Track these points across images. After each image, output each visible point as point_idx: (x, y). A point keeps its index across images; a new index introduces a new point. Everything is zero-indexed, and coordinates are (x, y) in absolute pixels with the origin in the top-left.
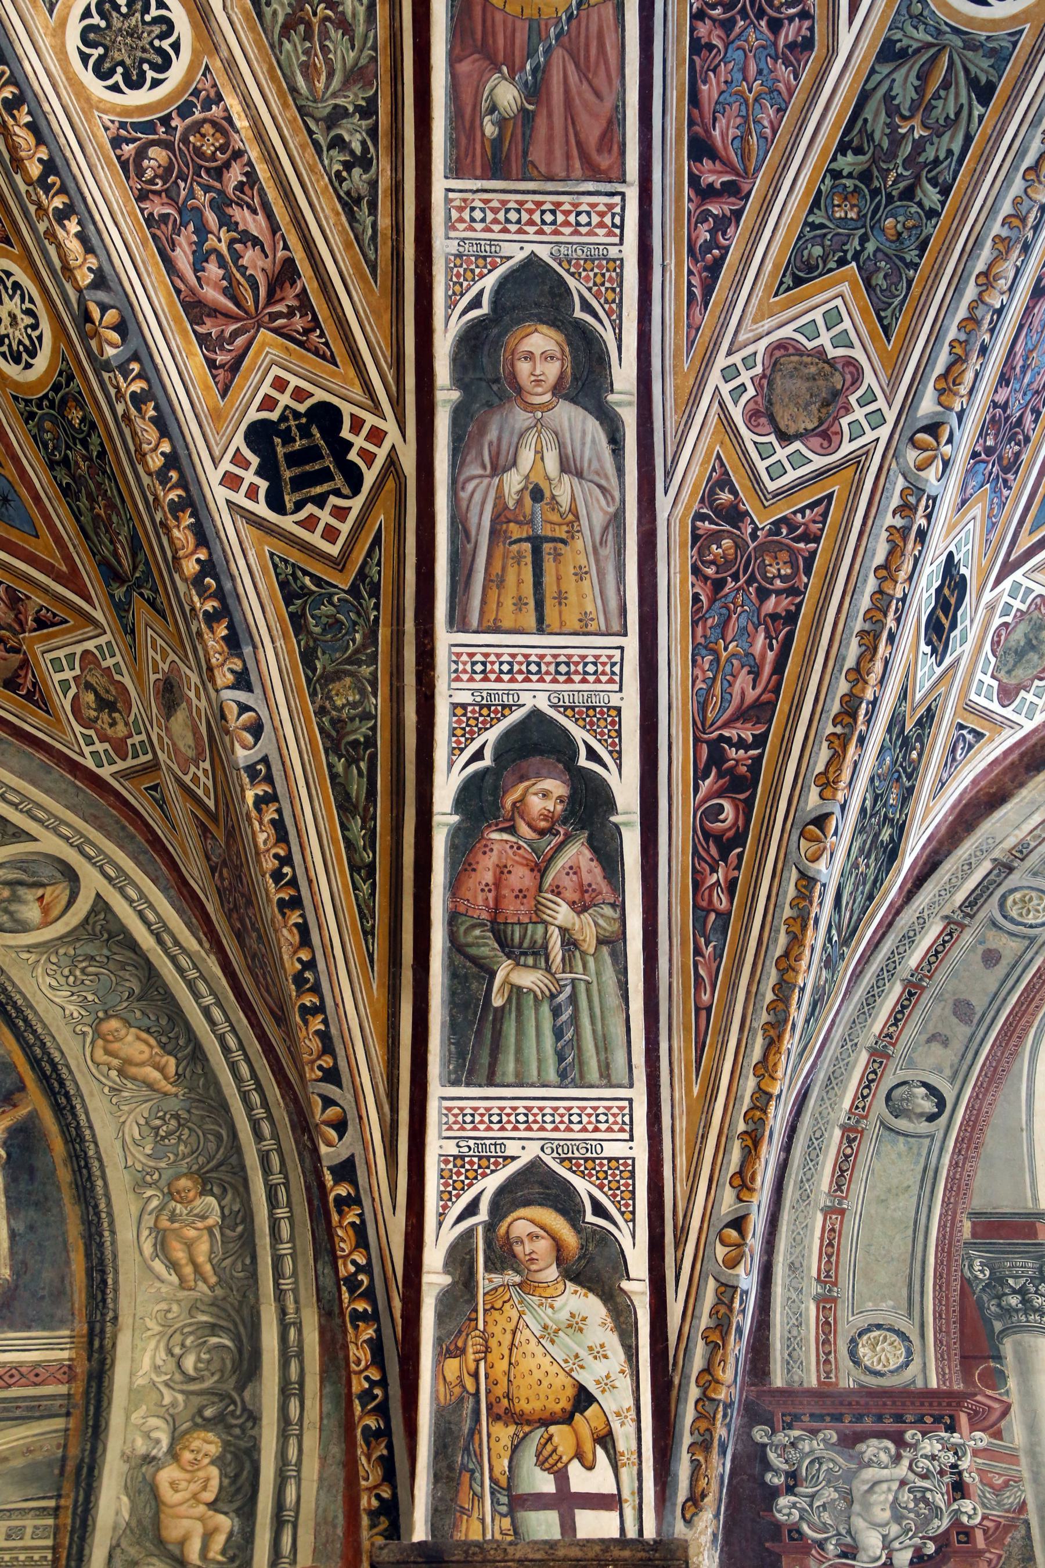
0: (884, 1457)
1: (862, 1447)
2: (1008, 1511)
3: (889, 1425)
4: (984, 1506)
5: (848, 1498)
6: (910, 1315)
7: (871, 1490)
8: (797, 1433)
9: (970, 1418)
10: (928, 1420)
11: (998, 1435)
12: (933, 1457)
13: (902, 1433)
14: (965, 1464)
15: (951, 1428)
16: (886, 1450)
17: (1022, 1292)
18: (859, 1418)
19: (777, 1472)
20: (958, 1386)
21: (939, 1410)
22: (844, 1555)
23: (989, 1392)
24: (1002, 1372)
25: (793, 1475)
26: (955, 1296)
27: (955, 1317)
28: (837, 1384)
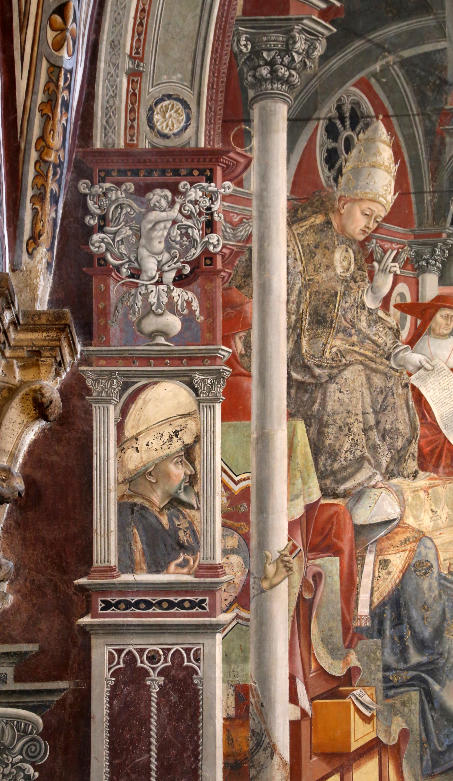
0: (164, 203)
1: (150, 195)
2: (239, 241)
3: (170, 178)
4: (224, 238)
5: (138, 234)
6: (192, 87)
7: (153, 228)
8: (108, 185)
9: (224, 170)
10: (196, 173)
11: (240, 184)
12: (196, 202)
13: (177, 183)
14: (216, 207)
15: (210, 180)
16: (166, 197)
17: (272, 63)
18: (150, 173)
19: (93, 215)
20: (218, 146)
21: (200, 164)
22: (132, 276)
23: (239, 150)
24: (249, 132)
25: (103, 218)
28: (137, 145)
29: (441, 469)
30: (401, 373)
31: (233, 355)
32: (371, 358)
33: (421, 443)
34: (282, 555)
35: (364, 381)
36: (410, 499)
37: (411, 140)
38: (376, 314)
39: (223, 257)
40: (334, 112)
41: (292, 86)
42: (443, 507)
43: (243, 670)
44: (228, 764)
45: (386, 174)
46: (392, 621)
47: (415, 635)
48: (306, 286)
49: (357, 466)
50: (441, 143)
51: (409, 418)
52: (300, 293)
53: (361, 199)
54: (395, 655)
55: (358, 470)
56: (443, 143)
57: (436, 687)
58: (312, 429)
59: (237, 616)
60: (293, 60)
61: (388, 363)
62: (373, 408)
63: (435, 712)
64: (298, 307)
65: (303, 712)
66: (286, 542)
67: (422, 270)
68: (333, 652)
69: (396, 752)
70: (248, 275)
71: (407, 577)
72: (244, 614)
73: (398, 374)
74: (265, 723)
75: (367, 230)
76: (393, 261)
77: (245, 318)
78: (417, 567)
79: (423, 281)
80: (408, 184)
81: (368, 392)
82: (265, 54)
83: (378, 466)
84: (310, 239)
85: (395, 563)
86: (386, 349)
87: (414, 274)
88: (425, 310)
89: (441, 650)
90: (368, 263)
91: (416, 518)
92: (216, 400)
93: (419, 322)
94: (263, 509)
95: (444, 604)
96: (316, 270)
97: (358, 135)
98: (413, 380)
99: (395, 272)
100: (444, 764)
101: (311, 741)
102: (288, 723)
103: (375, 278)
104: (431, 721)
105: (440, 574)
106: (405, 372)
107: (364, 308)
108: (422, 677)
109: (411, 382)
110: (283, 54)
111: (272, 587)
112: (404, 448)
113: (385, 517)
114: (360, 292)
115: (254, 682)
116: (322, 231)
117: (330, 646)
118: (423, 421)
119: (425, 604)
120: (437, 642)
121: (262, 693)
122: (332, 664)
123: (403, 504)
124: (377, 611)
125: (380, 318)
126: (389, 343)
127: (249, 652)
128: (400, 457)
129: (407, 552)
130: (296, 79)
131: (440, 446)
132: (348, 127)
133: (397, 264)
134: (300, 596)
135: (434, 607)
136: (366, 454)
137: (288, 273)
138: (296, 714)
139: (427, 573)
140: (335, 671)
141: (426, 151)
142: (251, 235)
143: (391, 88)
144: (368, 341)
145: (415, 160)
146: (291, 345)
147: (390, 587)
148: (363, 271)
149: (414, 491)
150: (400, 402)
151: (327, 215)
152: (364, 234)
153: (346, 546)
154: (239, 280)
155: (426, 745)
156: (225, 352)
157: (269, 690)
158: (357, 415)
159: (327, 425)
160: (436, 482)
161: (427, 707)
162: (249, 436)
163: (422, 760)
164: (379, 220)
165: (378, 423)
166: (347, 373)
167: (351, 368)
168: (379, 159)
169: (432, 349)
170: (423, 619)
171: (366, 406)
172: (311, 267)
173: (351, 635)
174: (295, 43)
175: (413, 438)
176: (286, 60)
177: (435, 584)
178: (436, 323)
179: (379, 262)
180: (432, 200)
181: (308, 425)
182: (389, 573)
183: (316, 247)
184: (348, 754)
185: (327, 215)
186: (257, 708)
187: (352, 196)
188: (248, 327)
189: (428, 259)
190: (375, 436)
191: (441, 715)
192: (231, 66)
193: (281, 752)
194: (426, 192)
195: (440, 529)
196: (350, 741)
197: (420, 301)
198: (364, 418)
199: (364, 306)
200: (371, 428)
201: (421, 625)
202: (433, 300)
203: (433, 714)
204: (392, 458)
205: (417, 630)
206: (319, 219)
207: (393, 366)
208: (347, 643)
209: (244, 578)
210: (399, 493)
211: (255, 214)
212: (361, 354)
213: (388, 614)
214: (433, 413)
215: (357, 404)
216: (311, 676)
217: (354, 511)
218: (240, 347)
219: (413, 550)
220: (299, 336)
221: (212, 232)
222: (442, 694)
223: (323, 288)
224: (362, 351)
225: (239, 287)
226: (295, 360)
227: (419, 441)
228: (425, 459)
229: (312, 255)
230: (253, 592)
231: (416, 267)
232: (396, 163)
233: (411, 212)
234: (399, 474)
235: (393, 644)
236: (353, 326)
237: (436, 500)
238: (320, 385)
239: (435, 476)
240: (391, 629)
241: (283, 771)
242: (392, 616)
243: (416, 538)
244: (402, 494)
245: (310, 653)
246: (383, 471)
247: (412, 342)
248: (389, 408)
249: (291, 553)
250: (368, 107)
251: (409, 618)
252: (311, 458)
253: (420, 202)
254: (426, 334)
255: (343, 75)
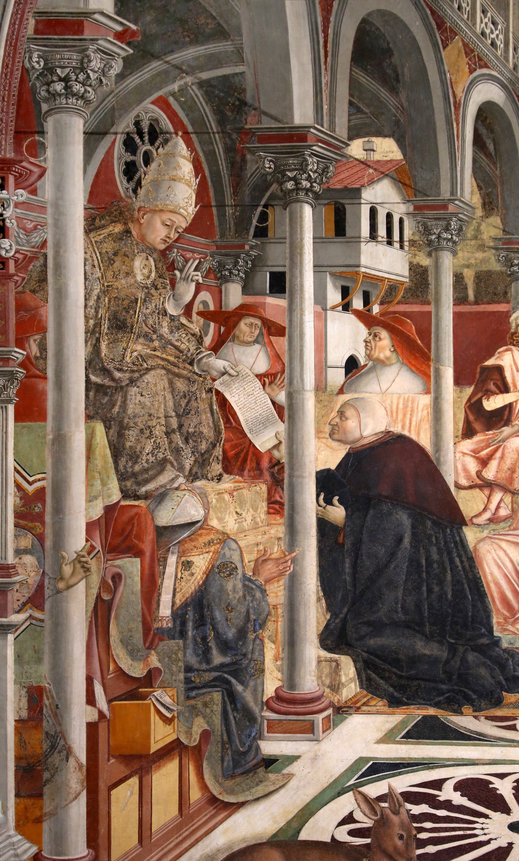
2: (33, 247)
4: (18, 243)
9: (16, 179)
11: (34, 192)
17: (66, 80)
23: (32, 160)
24: (43, 144)
26: (16, 83)
27: (14, 100)
29: (246, 473)
30: (205, 378)
31: (28, 357)
32: (174, 363)
33: (225, 447)
34: (79, 556)
35: (167, 385)
36: (214, 501)
37: (211, 155)
38: (179, 320)
39: (16, 262)
40: (132, 128)
41: (87, 102)
42: (248, 510)
43: (36, 671)
44: (20, 766)
45: (187, 187)
46: (195, 622)
47: (218, 636)
48: (105, 291)
49: (159, 469)
50: (242, 160)
51: (213, 421)
52: (99, 298)
53: (161, 211)
54: (198, 655)
55: (161, 472)
56: (244, 160)
57: (240, 688)
58: (112, 432)
59: (31, 617)
60: (88, 77)
61: (191, 368)
62: (175, 412)
63: (237, 712)
64: (97, 312)
65: (101, 714)
66: (84, 543)
67: (226, 280)
68: (133, 653)
69: (198, 753)
70: (43, 280)
71: (211, 578)
72: (38, 614)
73: (201, 379)
74: (60, 725)
75: (167, 239)
76: (195, 270)
77: (40, 321)
78: (221, 569)
79: (226, 290)
80: (209, 198)
81: (171, 396)
82: (59, 71)
83: (181, 469)
84: (109, 247)
85: (198, 564)
86: (189, 355)
87: (217, 283)
88: (228, 318)
89: (244, 651)
90: (169, 271)
91: (220, 520)
92: (9, 401)
93: (222, 329)
94: (59, 509)
95: (248, 605)
96: (115, 276)
97: (157, 150)
98: (218, 385)
99: (197, 281)
100: (245, 765)
101: (109, 743)
102: (85, 725)
103: (177, 286)
104: (233, 722)
105: (244, 575)
106: (208, 378)
107: (166, 315)
108: (224, 678)
109: (215, 387)
110: (78, 71)
111: (69, 587)
112: (208, 451)
113: (188, 518)
114: (162, 298)
115: (48, 683)
116: (121, 239)
117: (129, 647)
118: (228, 425)
119: (229, 605)
120: (241, 643)
121: (57, 694)
122: (131, 665)
123: (207, 506)
124: (179, 612)
125: (182, 324)
126: (192, 349)
127: (43, 653)
128: (204, 460)
129: (211, 554)
130: (91, 95)
131: (245, 450)
132: (147, 141)
133: (199, 273)
134: (99, 597)
135: (238, 608)
136: (169, 457)
137: (86, 279)
138: (92, 715)
139: (231, 574)
140: (135, 673)
141: (227, 167)
142: (46, 241)
143: (190, 107)
144: (170, 346)
145: (216, 175)
146: (90, 348)
147: (193, 588)
148: (164, 278)
149: (219, 494)
150: (203, 406)
151: (126, 224)
152: (164, 244)
153: (147, 547)
154: (33, 284)
155: (227, 746)
156: (19, 354)
157: (65, 692)
158: (159, 418)
159: (128, 428)
160: (241, 485)
161: (229, 708)
162: (44, 437)
163: (223, 761)
164: (180, 230)
165: (180, 426)
166: (149, 377)
167: (153, 372)
168: (180, 173)
169: (236, 356)
170: (227, 620)
171: (169, 410)
172: (110, 274)
173: (152, 635)
174: (90, 61)
175: (218, 442)
176: (81, 77)
177: (240, 585)
178: (241, 331)
179: (181, 271)
180: (234, 214)
181: (108, 428)
182: (192, 574)
183: (115, 254)
184: (147, 756)
185: (126, 224)
186: (51, 710)
187: (152, 207)
188: (43, 330)
189: (231, 269)
190: (178, 439)
191: (243, 716)
192: (22, 81)
193: (77, 755)
194: (228, 206)
195: (245, 531)
196: (149, 743)
197: (223, 309)
198: (166, 421)
199: (165, 313)
200: (173, 431)
201: (225, 625)
202: (237, 308)
203: (235, 715)
204: (195, 461)
205: (220, 631)
206: (118, 228)
207: (197, 371)
208: (147, 645)
209: (39, 578)
210: (203, 496)
211: (50, 221)
212: (163, 359)
213: (190, 615)
214: (238, 418)
215: (159, 407)
216: (109, 677)
217: (156, 513)
218: (35, 350)
219: (217, 552)
220: (98, 340)
221: (4, 237)
222: (245, 694)
223: (122, 295)
224: (164, 356)
225: (33, 291)
226: (93, 363)
227: (224, 445)
228: (230, 462)
229: (111, 262)
230: (47, 592)
231: (219, 276)
232: (197, 177)
233: (212, 223)
234: (203, 476)
235: (195, 645)
236: (155, 332)
237: (241, 503)
238: (120, 388)
239: (240, 478)
240: (193, 630)
241: (79, 774)
242: (195, 617)
243: (220, 540)
244: (206, 497)
245: (109, 654)
246: (187, 473)
247: (216, 348)
248: (193, 412)
249: (89, 553)
250: (166, 124)
251: (213, 619)
252: (110, 460)
253: (222, 215)
254: (230, 341)
255: (140, 93)
